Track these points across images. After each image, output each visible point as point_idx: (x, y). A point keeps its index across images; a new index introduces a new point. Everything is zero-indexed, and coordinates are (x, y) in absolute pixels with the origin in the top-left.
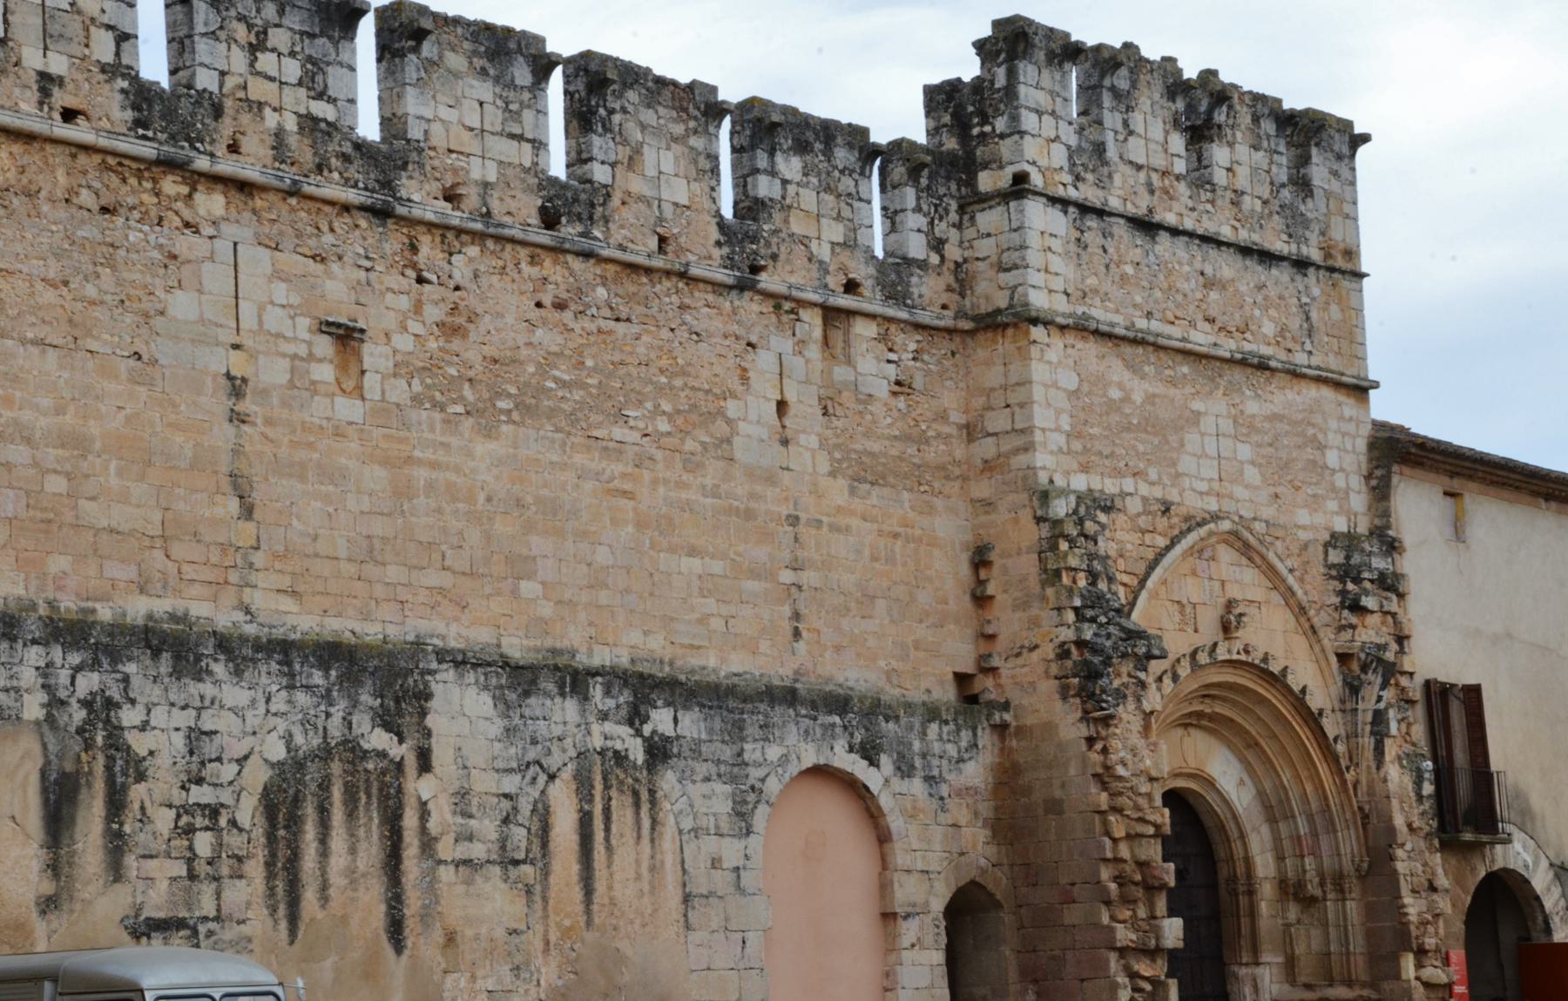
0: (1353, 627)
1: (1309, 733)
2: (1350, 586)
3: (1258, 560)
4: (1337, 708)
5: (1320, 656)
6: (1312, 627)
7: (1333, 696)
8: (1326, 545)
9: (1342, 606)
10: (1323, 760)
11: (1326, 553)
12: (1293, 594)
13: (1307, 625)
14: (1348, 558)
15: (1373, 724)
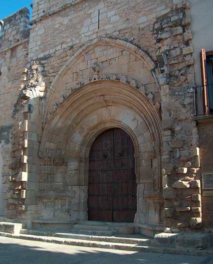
6: (141, 56)
11: (154, 27)
13: (139, 57)
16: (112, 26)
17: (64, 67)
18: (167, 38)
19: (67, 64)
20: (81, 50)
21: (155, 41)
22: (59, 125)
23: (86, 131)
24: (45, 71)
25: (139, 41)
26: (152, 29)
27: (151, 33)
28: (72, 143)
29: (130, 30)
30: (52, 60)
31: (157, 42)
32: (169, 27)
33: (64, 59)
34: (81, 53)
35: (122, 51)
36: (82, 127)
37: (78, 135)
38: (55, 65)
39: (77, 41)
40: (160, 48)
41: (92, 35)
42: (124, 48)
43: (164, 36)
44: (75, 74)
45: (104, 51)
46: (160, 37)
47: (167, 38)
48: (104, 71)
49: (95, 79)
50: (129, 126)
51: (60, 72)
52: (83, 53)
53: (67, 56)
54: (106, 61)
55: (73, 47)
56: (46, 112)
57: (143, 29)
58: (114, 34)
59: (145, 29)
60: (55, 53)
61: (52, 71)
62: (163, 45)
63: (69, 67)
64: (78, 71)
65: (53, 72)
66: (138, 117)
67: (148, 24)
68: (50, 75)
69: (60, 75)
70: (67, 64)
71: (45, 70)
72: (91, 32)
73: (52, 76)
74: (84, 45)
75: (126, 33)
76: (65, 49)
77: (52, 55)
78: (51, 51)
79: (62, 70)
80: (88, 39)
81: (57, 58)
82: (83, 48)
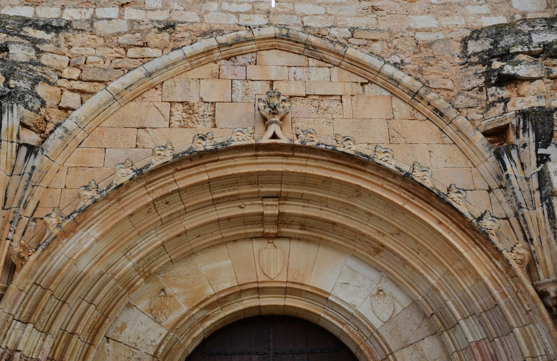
0: (505, 101)
1: (440, 216)
2: (496, 64)
3: (333, 58)
4: (494, 184)
5: (457, 138)
6: (436, 110)
7: (486, 174)
8: (465, 42)
9: (488, 83)
10: (471, 243)
11: (465, 46)
12: (398, 83)
13: (428, 110)
14: (495, 43)
15: (540, 189)
16: (321, 10)
17: (138, 73)
18: (532, 80)
19: (150, 66)
20: (211, 42)
21: (481, 82)
22: (84, 265)
23: (185, 309)
24: (43, 65)
25: (420, 71)
26: (458, 51)
27: (458, 60)
28: (109, 346)
29: (386, 36)
30: (77, 39)
31: (488, 83)
32: (530, 53)
33: (132, 52)
34: (209, 52)
35: (362, 84)
36: (163, 290)
37: (144, 318)
38: (90, 59)
39: (191, 16)
40: (505, 101)
41: (248, 13)
42: (371, 76)
43: (522, 71)
44: (180, 107)
45: (299, 70)
46: (512, 72)
47: (532, 80)
48: (297, 124)
49: (274, 136)
50: (360, 310)
51: (116, 85)
52: (217, 54)
53: (145, 45)
54: (307, 96)
55: (173, 26)
56: (31, 207)
57: (429, 45)
58: (333, 31)
59: (434, 47)
60: (92, 21)
61: (76, 73)
62: (519, 95)
63: (156, 79)
64: (194, 100)
65: (79, 79)
66: (388, 287)
67: (441, 36)
68: (61, 82)
69: (116, 96)
70: (150, 66)
71: (43, 61)
72: (247, 7)
73: (73, 91)
74: (220, 32)
75: (374, 40)
76: (131, 22)
77: (75, 25)
78: (70, 14)
79: (128, 79)
80: (233, 20)
81: (101, 41)
82: (222, 39)
